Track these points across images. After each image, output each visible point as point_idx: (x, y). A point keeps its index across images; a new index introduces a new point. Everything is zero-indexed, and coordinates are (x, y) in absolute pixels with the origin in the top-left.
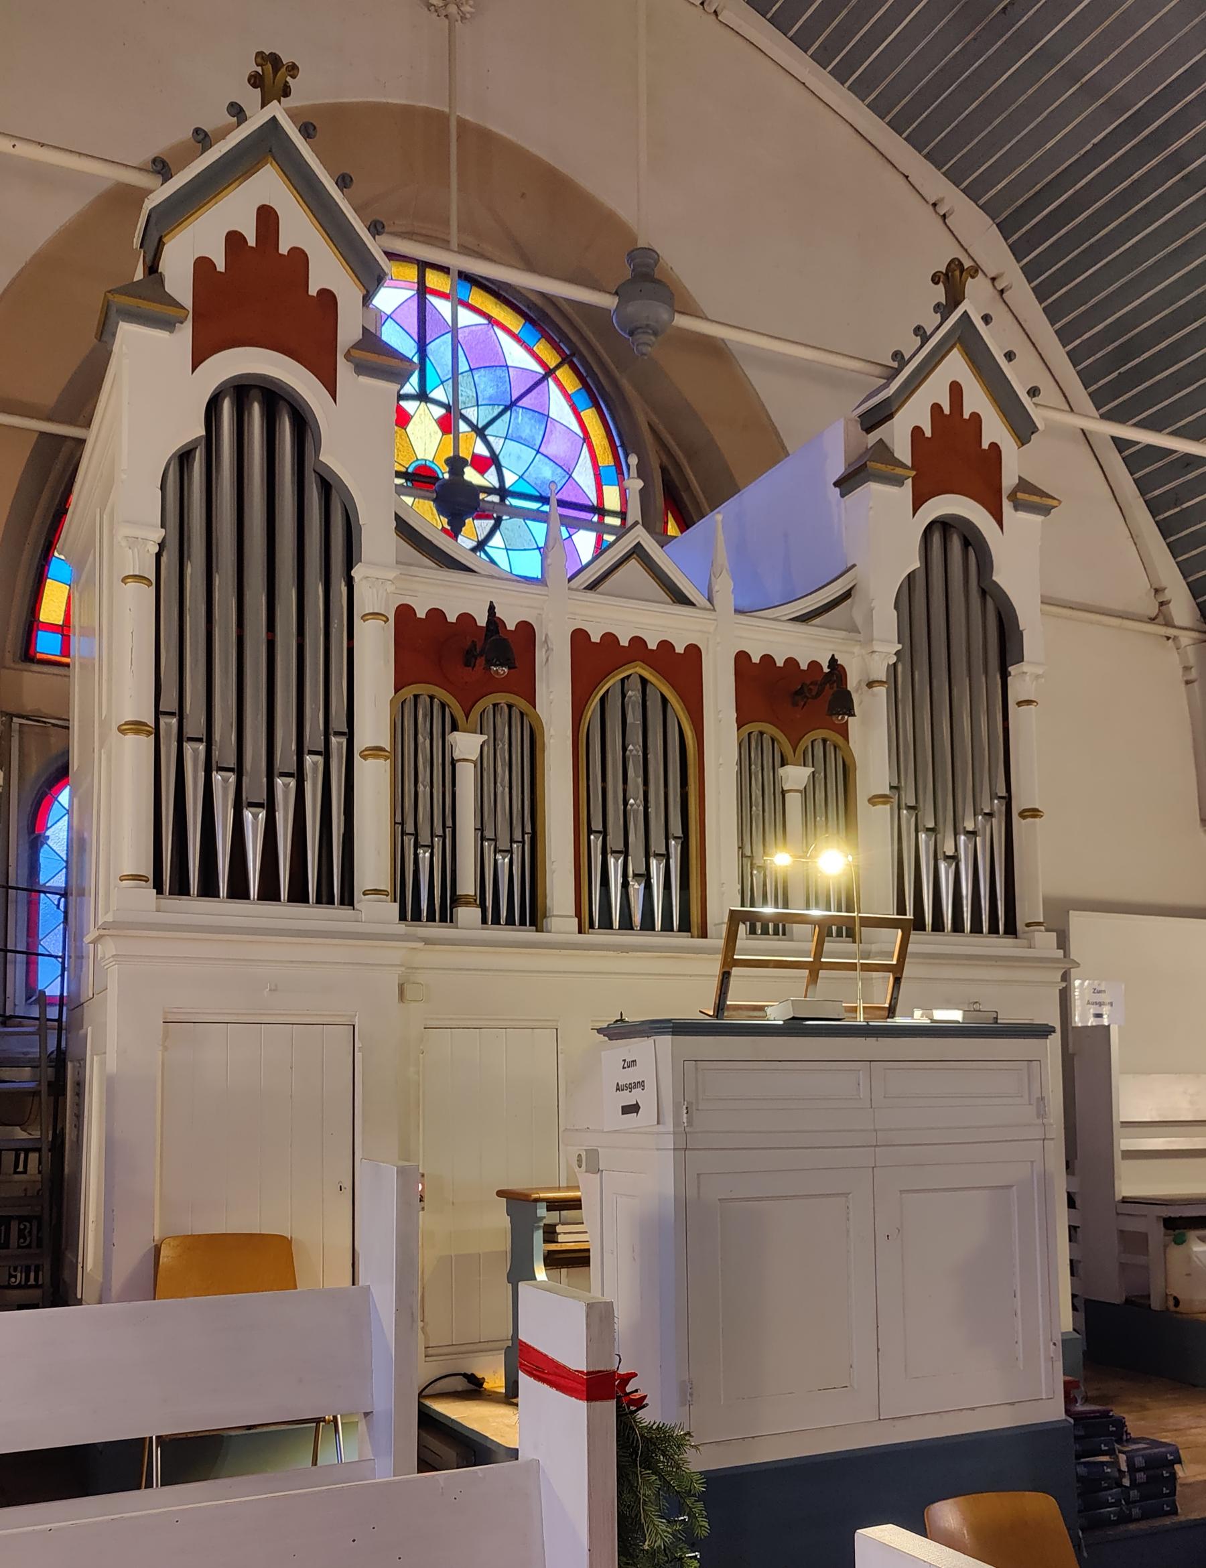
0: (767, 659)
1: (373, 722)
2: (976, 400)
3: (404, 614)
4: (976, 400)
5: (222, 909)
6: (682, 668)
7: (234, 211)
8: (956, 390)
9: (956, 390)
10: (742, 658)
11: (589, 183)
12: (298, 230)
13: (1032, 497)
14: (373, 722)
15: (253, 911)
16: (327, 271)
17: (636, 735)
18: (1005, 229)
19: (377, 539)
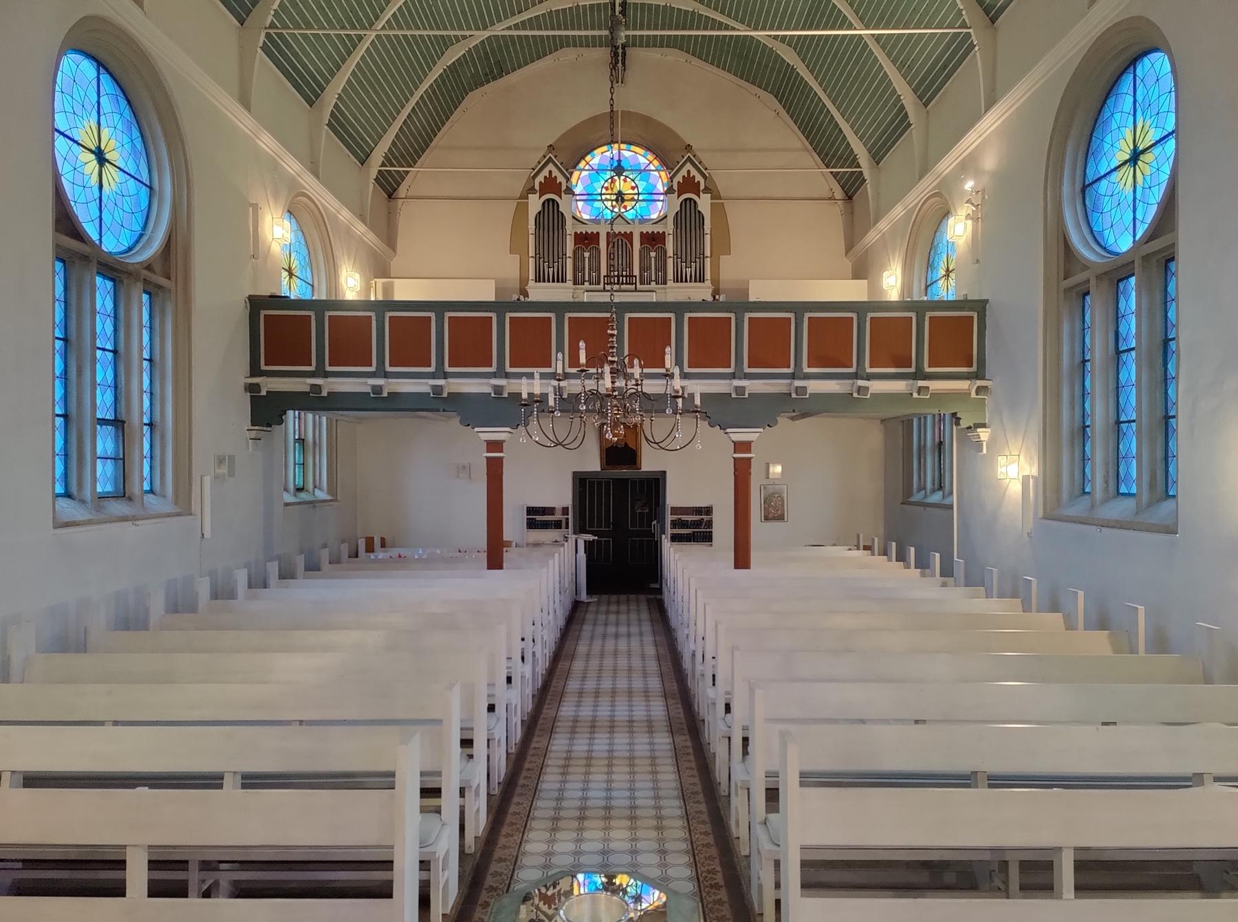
1: (569, 253)
2: (694, 172)
4: (694, 172)
5: (546, 284)
6: (629, 237)
7: (545, 173)
8: (689, 172)
9: (689, 172)
11: (655, 117)
12: (556, 173)
13: (707, 190)
14: (569, 253)
15: (551, 284)
16: (560, 179)
18: (776, 97)
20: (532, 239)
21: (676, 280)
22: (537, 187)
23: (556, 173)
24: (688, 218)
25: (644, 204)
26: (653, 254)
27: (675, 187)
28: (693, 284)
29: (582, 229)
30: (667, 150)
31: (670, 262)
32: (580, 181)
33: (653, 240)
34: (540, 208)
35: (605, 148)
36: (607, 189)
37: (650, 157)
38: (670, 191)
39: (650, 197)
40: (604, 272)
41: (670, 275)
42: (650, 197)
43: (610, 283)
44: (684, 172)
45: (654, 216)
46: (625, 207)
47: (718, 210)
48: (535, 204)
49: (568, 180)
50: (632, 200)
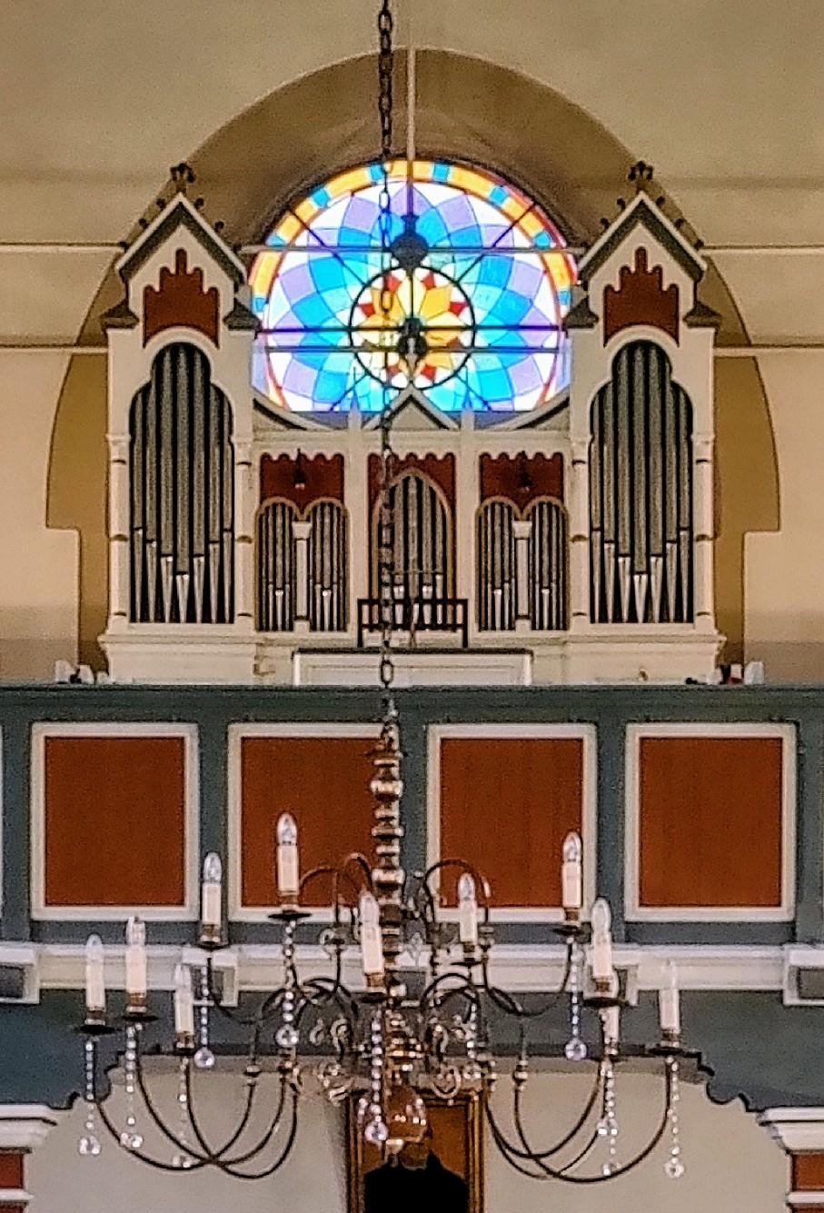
0: (504, 456)
1: (244, 523)
2: (658, 256)
3: (265, 458)
4: (658, 256)
6: (442, 470)
8: (641, 254)
9: (641, 254)
10: (485, 457)
12: (198, 257)
13: (702, 315)
14: (244, 523)
16: (214, 277)
17: (413, 514)
19: (243, 420)
20: (119, 478)
21: (600, 614)
22: (137, 306)
23: (198, 257)
24: (638, 410)
25: (492, 361)
26: (522, 528)
27: (597, 306)
28: (656, 628)
29: (285, 445)
30: (570, 179)
31: (579, 555)
32: (279, 283)
33: (523, 482)
34: (145, 376)
35: (364, 175)
36: (368, 310)
37: (513, 203)
38: (579, 317)
39: (513, 339)
40: (358, 587)
41: (580, 599)
42: (513, 339)
43: (381, 626)
44: (624, 256)
45: (527, 401)
46: (429, 372)
47: (740, 381)
48: (130, 359)
49: (239, 281)
50: (454, 346)
